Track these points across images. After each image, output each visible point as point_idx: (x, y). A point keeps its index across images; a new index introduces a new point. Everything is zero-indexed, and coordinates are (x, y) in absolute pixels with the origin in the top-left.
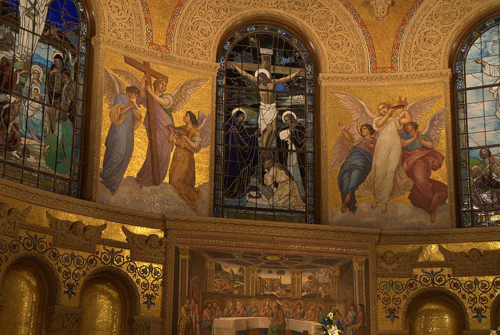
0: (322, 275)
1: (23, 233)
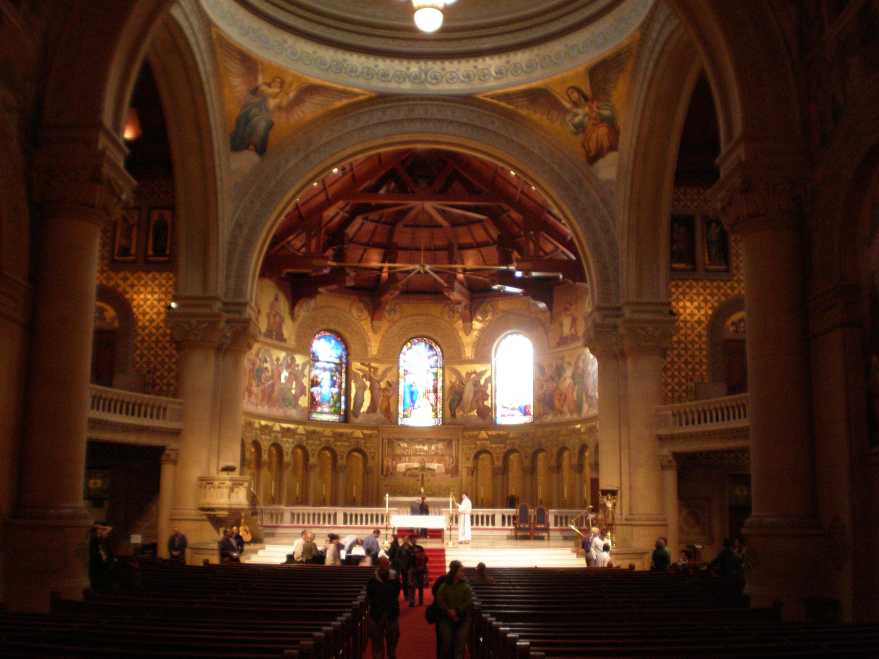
0: (441, 446)
1: (323, 439)
